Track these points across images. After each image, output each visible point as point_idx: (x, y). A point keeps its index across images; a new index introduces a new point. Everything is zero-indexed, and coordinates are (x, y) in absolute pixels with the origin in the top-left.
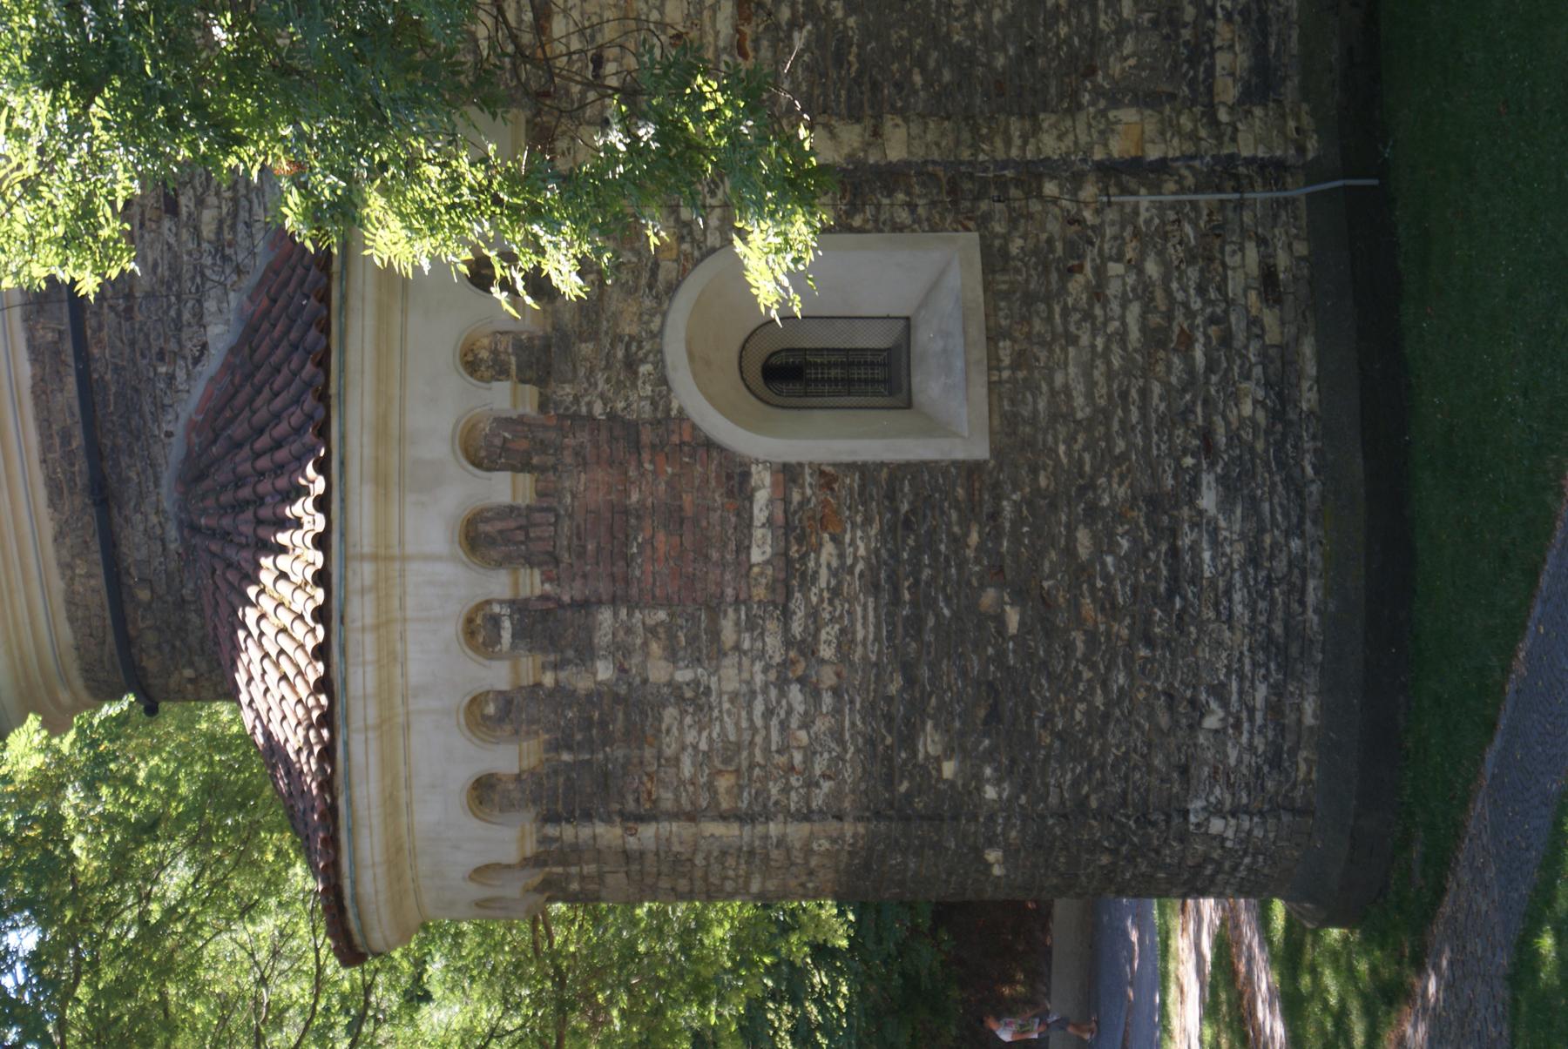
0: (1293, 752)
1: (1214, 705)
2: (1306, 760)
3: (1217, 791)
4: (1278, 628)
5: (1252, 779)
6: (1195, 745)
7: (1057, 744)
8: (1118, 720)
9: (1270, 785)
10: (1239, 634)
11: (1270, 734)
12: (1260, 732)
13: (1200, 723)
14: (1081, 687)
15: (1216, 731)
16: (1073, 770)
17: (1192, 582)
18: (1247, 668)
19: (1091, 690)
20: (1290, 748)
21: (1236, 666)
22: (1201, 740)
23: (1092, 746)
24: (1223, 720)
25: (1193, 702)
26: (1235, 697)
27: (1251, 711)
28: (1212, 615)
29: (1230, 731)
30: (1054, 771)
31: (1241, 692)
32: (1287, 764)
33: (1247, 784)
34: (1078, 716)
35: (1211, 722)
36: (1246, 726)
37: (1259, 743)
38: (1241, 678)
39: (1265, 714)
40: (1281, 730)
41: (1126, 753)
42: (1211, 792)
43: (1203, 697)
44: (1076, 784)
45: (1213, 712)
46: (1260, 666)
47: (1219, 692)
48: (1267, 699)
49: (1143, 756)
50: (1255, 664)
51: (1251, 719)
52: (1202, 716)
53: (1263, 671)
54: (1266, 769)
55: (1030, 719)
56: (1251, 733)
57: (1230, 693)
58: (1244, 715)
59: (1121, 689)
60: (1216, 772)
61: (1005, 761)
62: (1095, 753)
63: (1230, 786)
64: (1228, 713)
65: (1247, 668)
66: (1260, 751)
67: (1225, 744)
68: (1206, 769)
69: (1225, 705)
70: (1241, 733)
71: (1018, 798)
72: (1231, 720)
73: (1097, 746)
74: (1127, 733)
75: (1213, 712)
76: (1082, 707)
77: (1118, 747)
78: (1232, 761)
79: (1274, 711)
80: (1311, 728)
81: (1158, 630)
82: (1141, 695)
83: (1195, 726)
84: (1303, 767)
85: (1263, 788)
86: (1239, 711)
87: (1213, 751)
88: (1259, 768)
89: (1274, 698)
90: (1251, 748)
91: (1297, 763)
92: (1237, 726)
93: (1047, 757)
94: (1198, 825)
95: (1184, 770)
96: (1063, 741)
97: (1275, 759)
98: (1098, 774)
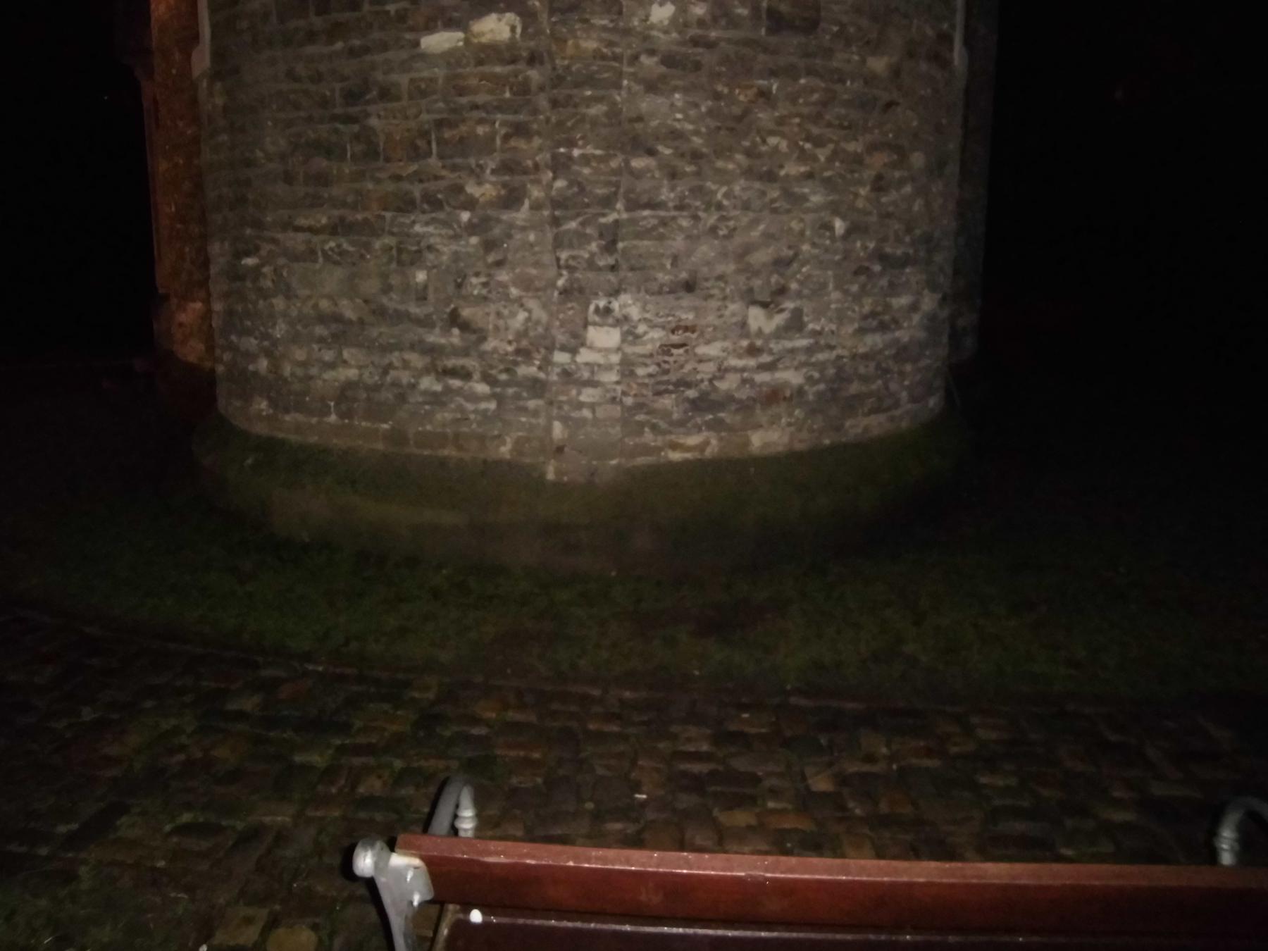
0: (717, 425)
1: (779, 319)
2: (706, 443)
3: (657, 334)
4: (854, 388)
5: (673, 377)
6: (725, 298)
7: (736, 110)
8: (763, 193)
9: (667, 402)
10: (849, 343)
11: (743, 394)
12: (744, 381)
13: (754, 303)
14: (808, 146)
15: (744, 324)
16: (697, 133)
17: (892, 285)
18: (821, 357)
19: (804, 157)
20: (722, 421)
21: (822, 342)
22: (733, 307)
23: (730, 159)
24: (760, 333)
25: (782, 291)
26: (789, 344)
27: (770, 367)
28: (867, 309)
29: (745, 343)
30: (696, 106)
31: (792, 351)
32: (699, 420)
33: (667, 372)
34: (773, 141)
35: (756, 318)
36: (752, 362)
37: (727, 384)
38: (809, 350)
39: (766, 384)
40: (746, 407)
41: (720, 207)
42: (654, 326)
43: (789, 305)
44: (675, 135)
45: (770, 317)
46: (822, 372)
47: (795, 324)
48: (786, 384)
49: (713, 230)
50: (821, 366)
51: (763, 367)
52: (765, 305)
53: (816, 375)
54: (692, 393)
55: (773, 73)
56: (743, 370)
57: (790, 339)
58: (766, 358)
59: (804, 198)
60: (686, 329)
61: (713, 34)
62: (720, 164)
63: (666, 349)
64: (768, 339)
65: (821, 357)
66: (717, 383)
67: (725, 338)
68: (691, 316)
69: (779, 334)
70: (740, 357)
71: (652, 52)
72: (759, 343)
73: (731, 166)
74: (746, 207)
75: (770, 317)
76: (784, 145)
77: (726, 195)
78: (702, 350)
79: (774, 396)
80: (747, 443)
81: (859, 244)
82: (795, 225)
83: (750, 299)
84: (693, 440)
85: (659, 394)
86: (771, 352)
87: (717, 322)
88: (688, 385)
89: (788, 394)
90: (723, 371)
91: (700, 430)
92: (753, 351)
93: (717, 96)
94: (608, 311)
95: (689, 287)
96: (739, 119)
97: (705, 404)
98: (689, 169)
